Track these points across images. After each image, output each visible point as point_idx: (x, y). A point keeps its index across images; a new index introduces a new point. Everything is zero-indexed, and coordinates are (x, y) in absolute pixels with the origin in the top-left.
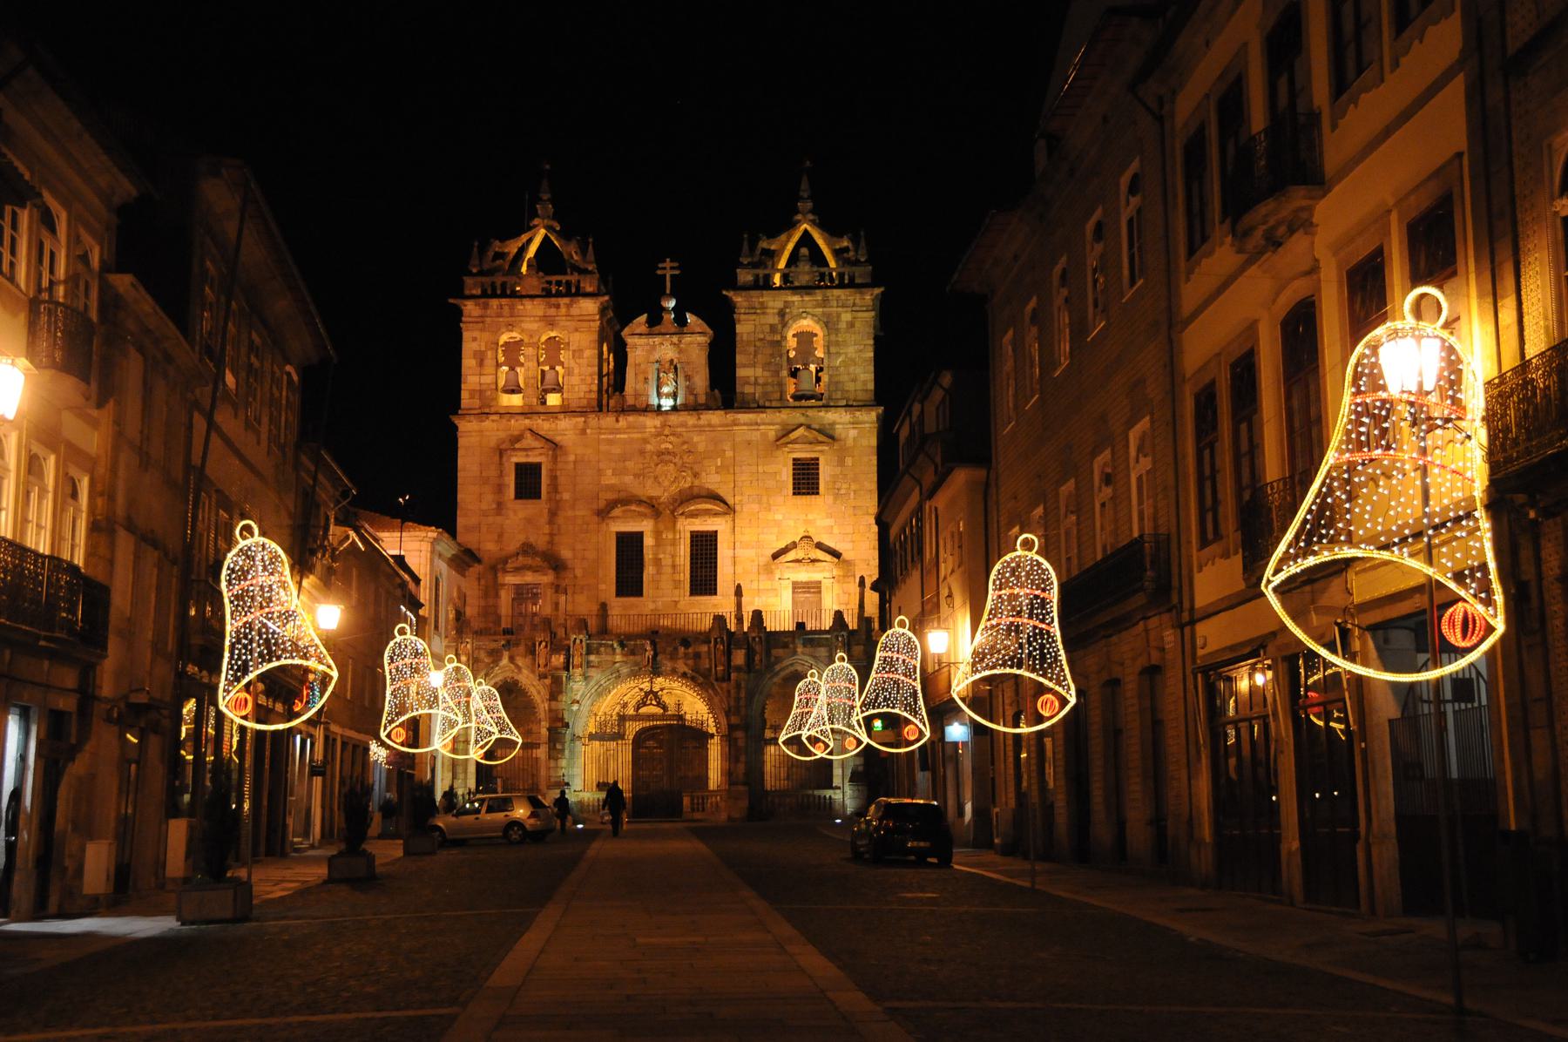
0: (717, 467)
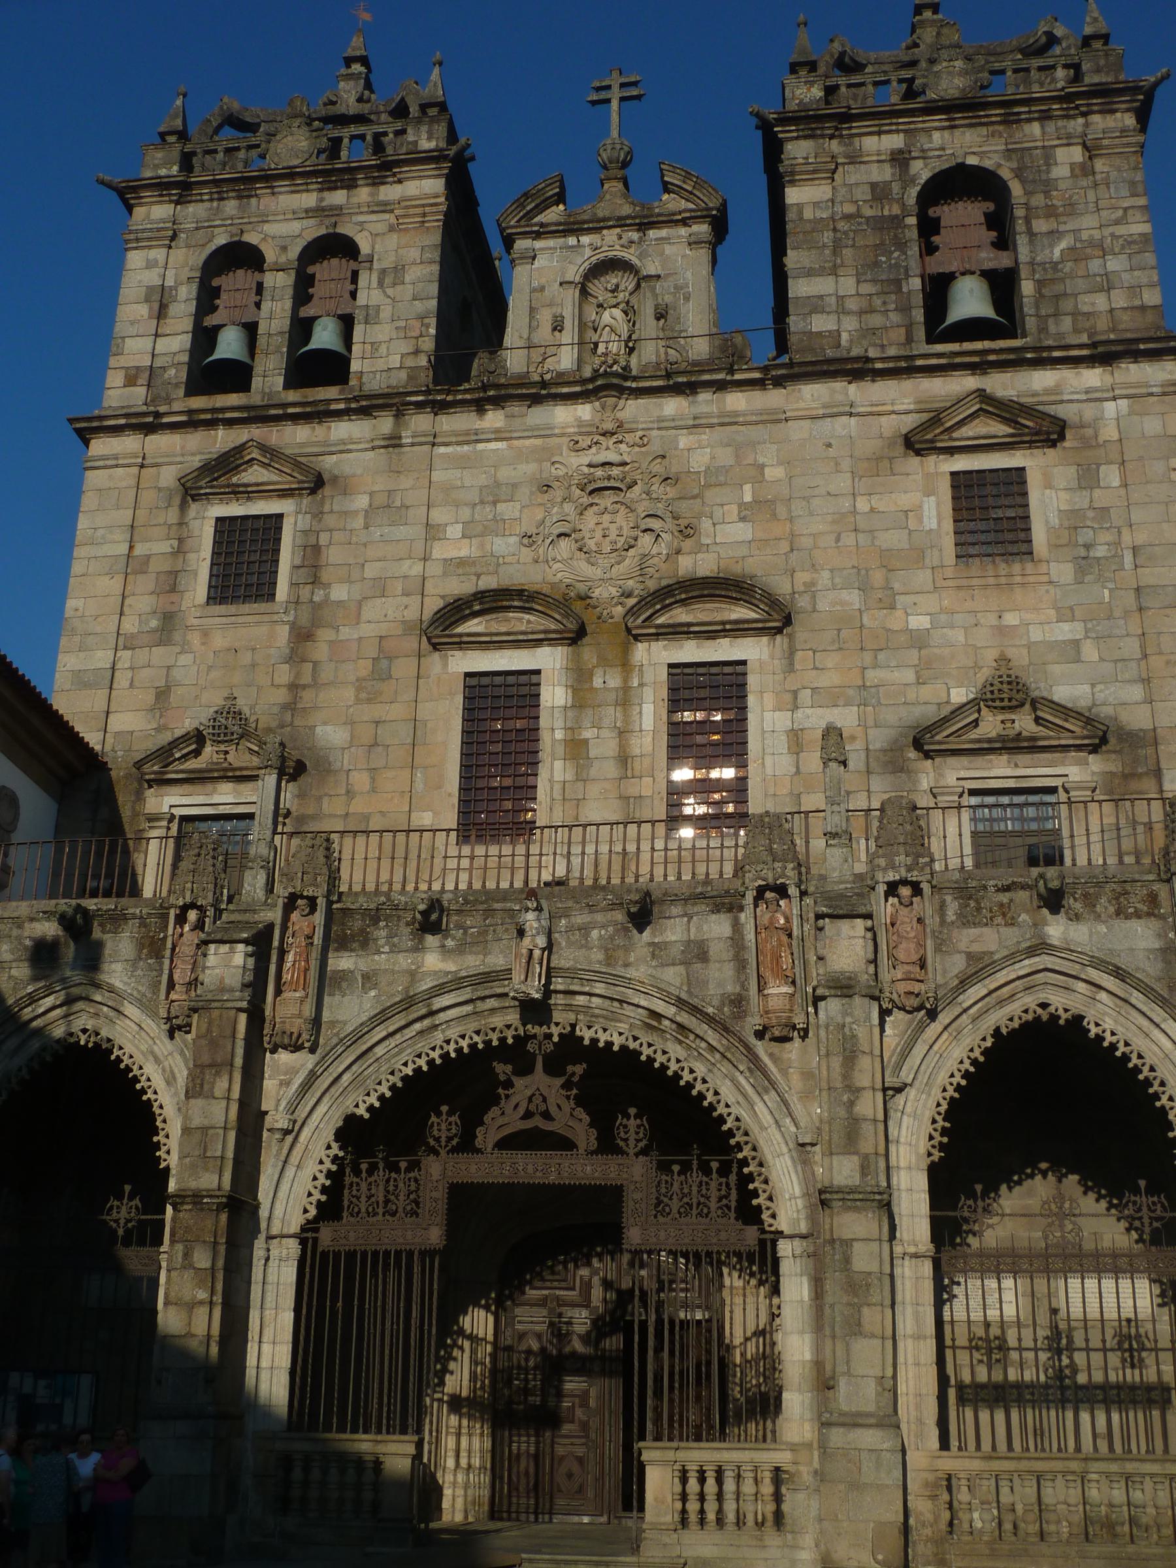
0: (742, 506)
